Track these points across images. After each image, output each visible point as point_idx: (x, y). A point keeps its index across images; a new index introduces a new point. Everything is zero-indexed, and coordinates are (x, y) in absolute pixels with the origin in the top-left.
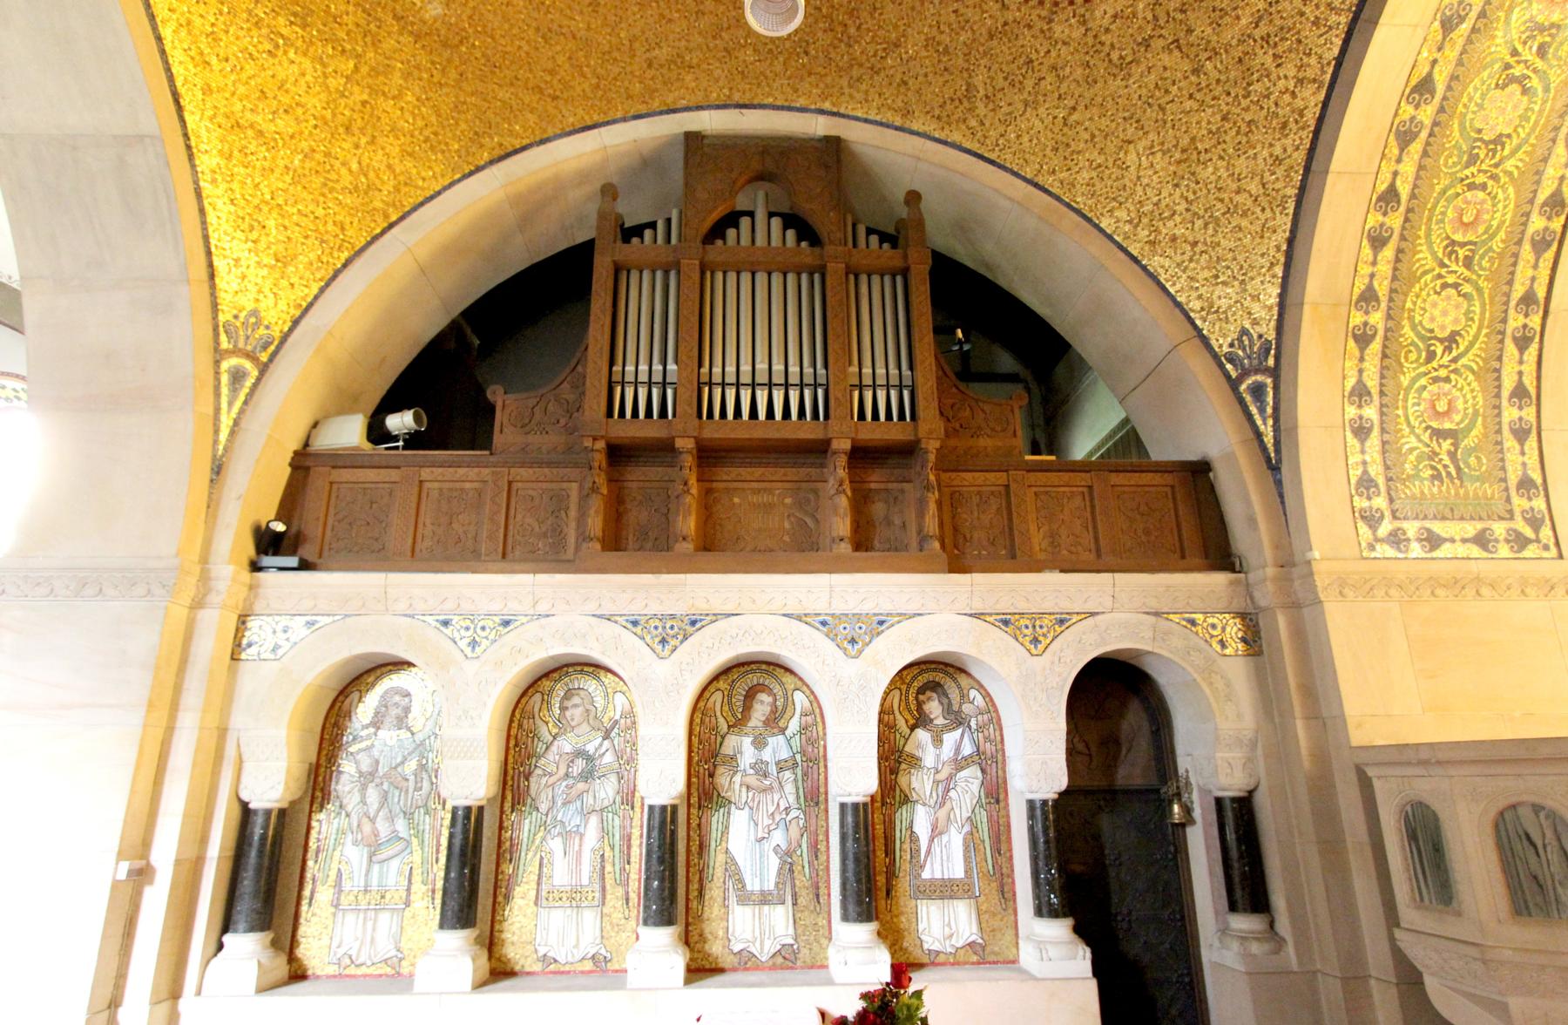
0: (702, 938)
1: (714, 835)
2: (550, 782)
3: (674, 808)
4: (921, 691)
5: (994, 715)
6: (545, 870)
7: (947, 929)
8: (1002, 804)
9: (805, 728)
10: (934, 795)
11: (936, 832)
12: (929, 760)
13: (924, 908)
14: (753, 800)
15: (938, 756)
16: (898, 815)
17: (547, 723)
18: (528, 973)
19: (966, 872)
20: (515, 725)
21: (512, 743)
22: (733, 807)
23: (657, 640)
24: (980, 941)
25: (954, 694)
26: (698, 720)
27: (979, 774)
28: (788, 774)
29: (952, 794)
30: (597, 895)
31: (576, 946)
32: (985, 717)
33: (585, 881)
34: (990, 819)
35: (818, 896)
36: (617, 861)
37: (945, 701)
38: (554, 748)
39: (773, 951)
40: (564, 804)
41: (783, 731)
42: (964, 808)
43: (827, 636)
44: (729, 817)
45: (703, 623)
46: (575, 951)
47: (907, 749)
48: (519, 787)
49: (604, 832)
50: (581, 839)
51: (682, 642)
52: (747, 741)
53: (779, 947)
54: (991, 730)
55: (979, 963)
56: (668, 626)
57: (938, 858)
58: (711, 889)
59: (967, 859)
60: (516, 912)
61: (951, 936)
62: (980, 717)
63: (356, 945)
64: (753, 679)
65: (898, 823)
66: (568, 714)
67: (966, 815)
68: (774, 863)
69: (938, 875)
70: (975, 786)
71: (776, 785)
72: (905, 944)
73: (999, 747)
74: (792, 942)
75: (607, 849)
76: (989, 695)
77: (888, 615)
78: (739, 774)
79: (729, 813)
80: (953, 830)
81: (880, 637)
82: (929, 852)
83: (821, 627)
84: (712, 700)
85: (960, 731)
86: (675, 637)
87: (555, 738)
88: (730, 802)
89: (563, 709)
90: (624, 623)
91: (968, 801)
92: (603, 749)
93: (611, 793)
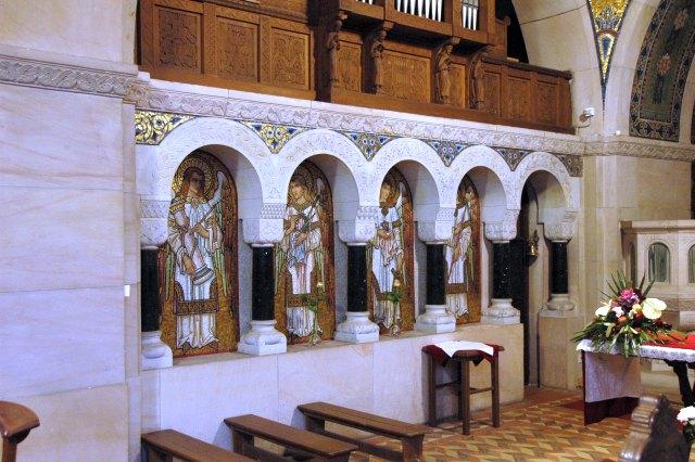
11: (454, 260)
28: (397, 230)
33: (309, 292)
40: (296, 246)
63: (191, 336)
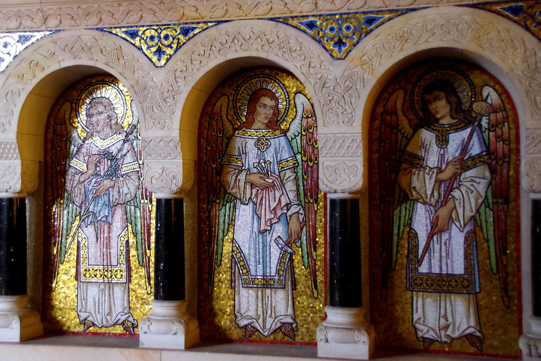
0: (213, 313)
1: (221, 227)
2: (82, 179)
3: (179, 202)
4: (428, 90)
5: (510, 113)
6: (82, 252)
7: (442, 321)
8: (512, 204)
9: (307, 129)
10: (436, 194)
12: (432, 160)
13: (420, 300)
14: (257, 196)
15: (442, 156)
16: (396, 212)
17: (76, 128)
18: (74, 333)
19: (466, 269)
20: (51, 130)
21: (49, 146)
22: (238, 203)
23: (154, 49)
24: (478, 334)
25: (465, 94)
26: (206, 124)
27: (487, 174)
29: (456, 193)
30: (124, 274)
31: (110, 314)
32: (500, 115)
34: (497, 220)
35: (315, 282)
36: (140, 248)
37: (454, 100)
38: (84, 150)
39: (273, 327)
40: (94, 198)
41: (285, 133)
42: (467, 208)
43: (313, 38)
44: (234, 211)
45: (197, 31)
46: (109, 318)
47: (409, 149)
48: (57, 183)
49: (128, 220)
50: (109, 228)
51: (177, 49)
52: (251, 143)
53: (279, 325)
54: (506, 129)
55: (475, 354)
56: (162, 36)
57: (437, 255)
58: (219, 273)
59: (467, 257)
60: (61, 284)
61: (447, 327)
62: (493, 116)
64: (256, 83)
65: (396, 220)
66: (94, 119)
67: (468, 214)
68: (275, 253)
69: (436, 270)
70: (482, 187)
71: (277, 183)
72: (399, 331)
73: (513, 146)
74: (291, 321)
75: (131, 236)
76: (506, 92)
77: (378, 12)
78: (244, 174)
79: (235, 207)
80: (455, 230)
81: (369, 36)
82: (427, 248)
83: (308, 30)
84: (218, 105)
85: (469, 130)
86: (170, 46)
87: (84, 142)
88: (236, 198)
89: (89, 116)
90: (124, 36)
91: (473, 200)
92: (124, 152)
93: (133, 190)
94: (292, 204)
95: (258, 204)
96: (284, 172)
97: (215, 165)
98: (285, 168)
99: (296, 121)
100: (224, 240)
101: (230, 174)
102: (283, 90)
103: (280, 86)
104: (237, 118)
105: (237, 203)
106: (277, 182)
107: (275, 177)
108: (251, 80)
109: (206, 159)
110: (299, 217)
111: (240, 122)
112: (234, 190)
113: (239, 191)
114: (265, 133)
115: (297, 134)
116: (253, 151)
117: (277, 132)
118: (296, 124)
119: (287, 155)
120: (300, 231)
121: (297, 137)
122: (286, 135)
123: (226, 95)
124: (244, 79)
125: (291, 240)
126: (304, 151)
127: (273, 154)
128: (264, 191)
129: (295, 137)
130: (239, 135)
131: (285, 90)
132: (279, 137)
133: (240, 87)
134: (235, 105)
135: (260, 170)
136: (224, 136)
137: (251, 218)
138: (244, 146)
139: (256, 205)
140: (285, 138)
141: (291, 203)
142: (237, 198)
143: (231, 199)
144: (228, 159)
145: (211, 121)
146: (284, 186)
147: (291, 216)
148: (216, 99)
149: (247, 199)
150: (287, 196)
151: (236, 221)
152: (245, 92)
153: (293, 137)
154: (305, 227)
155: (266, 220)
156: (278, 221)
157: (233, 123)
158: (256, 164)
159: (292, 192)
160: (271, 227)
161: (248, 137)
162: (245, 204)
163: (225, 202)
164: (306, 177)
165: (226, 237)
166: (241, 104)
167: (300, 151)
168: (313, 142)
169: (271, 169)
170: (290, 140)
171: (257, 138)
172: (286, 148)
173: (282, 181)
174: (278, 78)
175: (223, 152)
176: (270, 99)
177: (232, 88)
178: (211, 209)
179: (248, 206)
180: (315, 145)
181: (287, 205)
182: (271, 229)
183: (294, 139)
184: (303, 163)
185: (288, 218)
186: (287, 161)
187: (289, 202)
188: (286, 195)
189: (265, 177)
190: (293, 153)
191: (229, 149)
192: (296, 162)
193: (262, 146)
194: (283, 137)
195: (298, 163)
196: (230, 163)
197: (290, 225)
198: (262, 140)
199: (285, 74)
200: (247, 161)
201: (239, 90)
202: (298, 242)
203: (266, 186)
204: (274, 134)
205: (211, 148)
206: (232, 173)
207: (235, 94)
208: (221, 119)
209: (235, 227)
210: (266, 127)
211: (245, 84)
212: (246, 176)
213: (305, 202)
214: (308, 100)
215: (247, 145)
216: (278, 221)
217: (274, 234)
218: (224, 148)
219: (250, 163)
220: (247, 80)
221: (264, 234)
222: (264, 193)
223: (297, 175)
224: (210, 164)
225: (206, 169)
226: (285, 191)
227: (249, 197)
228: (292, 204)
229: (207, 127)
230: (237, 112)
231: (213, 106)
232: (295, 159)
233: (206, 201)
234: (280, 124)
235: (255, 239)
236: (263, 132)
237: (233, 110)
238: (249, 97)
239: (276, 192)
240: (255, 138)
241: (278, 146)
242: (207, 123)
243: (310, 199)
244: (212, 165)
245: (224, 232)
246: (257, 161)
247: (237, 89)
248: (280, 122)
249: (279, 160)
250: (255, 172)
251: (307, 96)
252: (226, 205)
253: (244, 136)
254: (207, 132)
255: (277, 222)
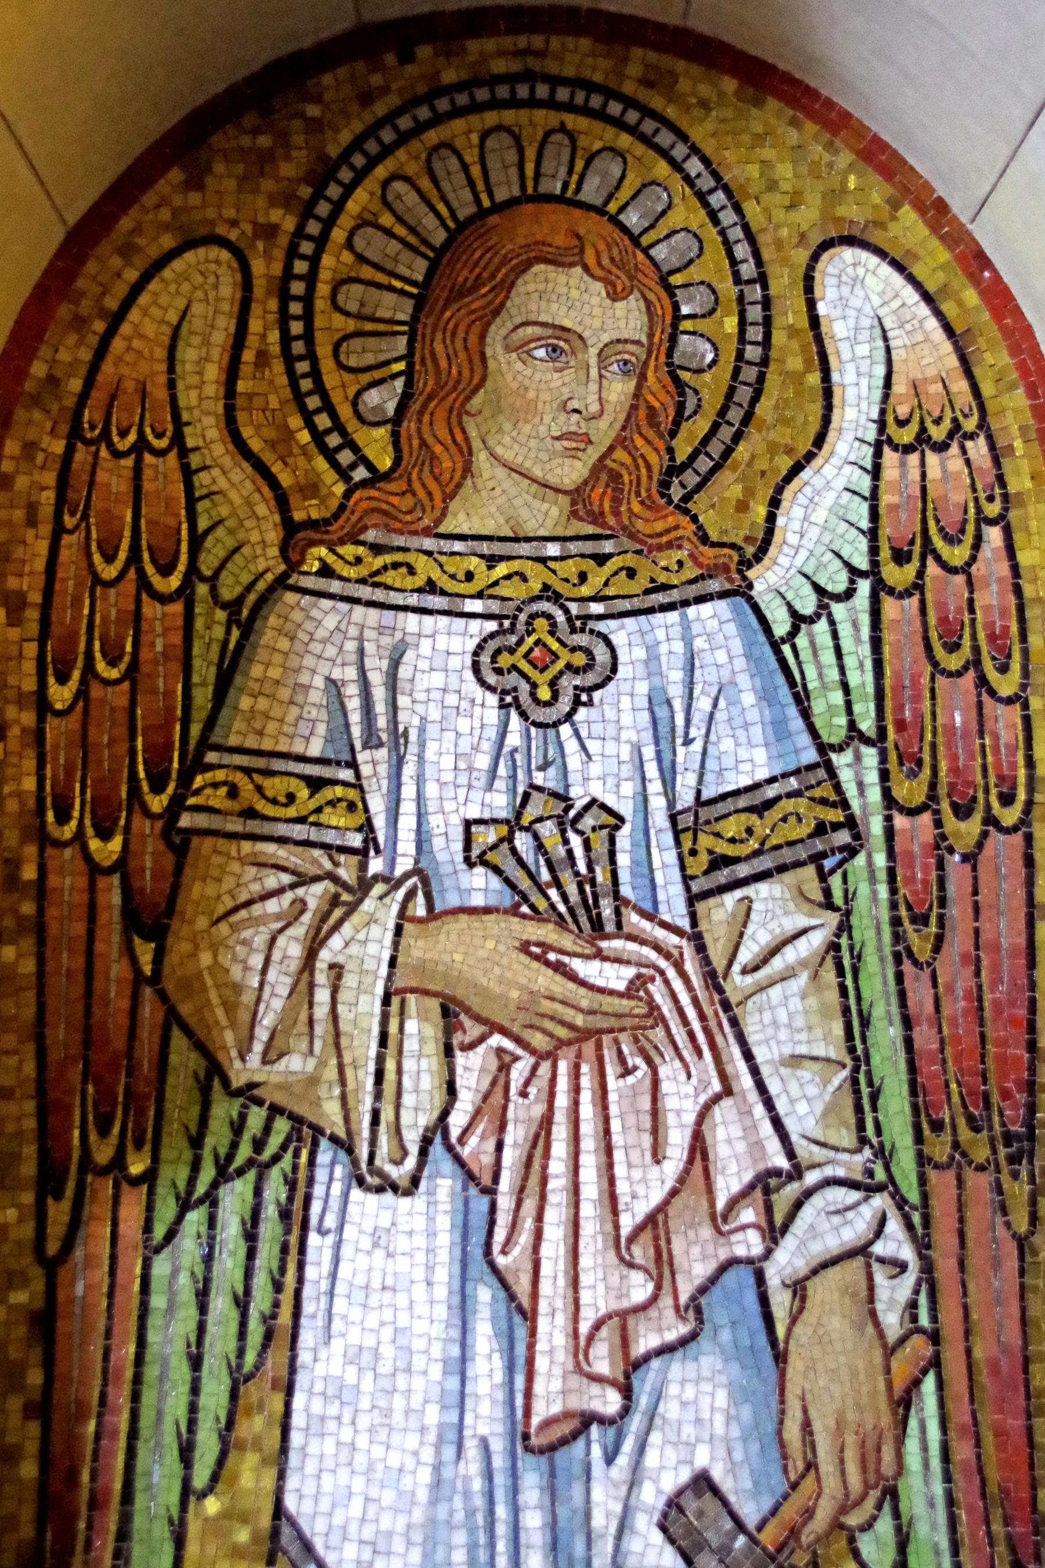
94: (811, 1178)
95: (505, 1184)
96: (730, 899)
97: (116, 844)
98: (743, 870)
99: (829, 471)
100: (194, 1528)
101: (256, 922)
102: (713, 216)
103: (689, 180)
104: (318, 437)
105: (321, 1175)
106: (678, 985)
107: (657, 948)
108: (438, 120)
109: (30, 784)
110: (871, 1299)
111: (344, 474)
112: (294, 1063)
113: (331, 1073)
114: (570, 569)
115: (839, 583)
116: (463, 725)
117: (669, 558)
118: (829, 498)
119: (760, 755)
120: (886, 1420)
121: (838, 610)
122: (743, 592)
123: (224, 243)
124: (380, 109)
125: (809, 1513)
126: (901, 725)
127: (637, 749)
128: (563, 1067)
129: (822, 606)
130: (335, 586)
131: (728, 217)
132: (686, 603)
133: (346, 175)
134: (297, 328)
135: (525, 884)
136: (202, 589)
137: (441, 1312)
138: (376, 679)
139: (490, 1191)
140: (735, 610)
141: (797, 1172)
142: (318, 1131)
143: (259, 1145)
144: (233, 792)
145: (82, 455)
146: (734, 1022)
147: (798, 1288)
148: (132, 275)
149: (412, 1139)
150: (759, 1110)
151: (307, 1338)
152: (387, 220)
153: (807, 605)
154: (929, 1384)
155: (584, 1328)
156: (693, 1336)
157: (285, 479)
158: (488, 836)
159: (806, 1073)
160: (627, 1392)
161: (413, 600)
162: (388, 1186)
163: (207, 1174)
164: (919, 942)
165: (212, 1505)
166: (351, 325)
167: (867, 725)
168: (976, 649)
169: (624, 876)
170: (781, 629)
171: (495, 607)
172: (748, 699)
173: (713, 979)
174: (671, 112)
175: (195, 730)
176: (599, 287)
177: (268, 185)
178: (68, 1243)
179: (418, 1202)
180: (992, 675)
181: (767, 1191)
182: (626, 1411)
183: (811, 620)
184: (900, 821)
185: (781, 1302)
186: (762, 808)
187: (782, 1162)
188: (753, 1097)
189: (567, 942)
190: (804, 739)
191: (245, 703)
192: (836, 815)
193: (542, 679)
194: (722, 606)
195: (851, 823)
196: (253, 826)
197: (795, 1366)
198: (541, 623)
199: (730, 85)
200: (408, 807)
201: (338, 207)
202: (868, 1526)
203: (579, 1020)
204: (642, 582)
205: (82, 693)
206: (272, 906)
207: (299, 233)
208: (178, 439)
209: (299, 1401)
210: (574, 514)
211: (387, 151)
212: (399, 930)
213: (922, 1160)
214: (927, 298)
215: (404, 672)
216: (693, 1336)
217: (651, 1459)
218: (203, 697)
219: (435, 821)
220: (405, 123)
221: (560, 1456)
222: (563, 1084)
223: (845, 927)
224: (69, 830)
225: (29, 873)
226: (742, 1066)
227: (424, 1120)
228: (811, 1178)
229: (47, 511)
230: (320, 388)
231: (100, 326)
232: (825, 791)
233: (29, 1169)
234: (687, 498)
235: (479, 1502)
236: (543, 560)
237: (278, 366)
238: (419, 269)
239: (669, 1070)
240: (475, 606)
241: (676, 676)
242: (50, 478)
243: (965, 1134)
244: (94, 844)
245: (186, 1453)
246: (500, 803)
247: (319, 194)
248: (691, 479)
249: (685, 798)
250: (478, 900)
251: (918, 270)
252: (211, 1199)
253: (379, 595)
254: (42, 547)
255: (683, 1342)
